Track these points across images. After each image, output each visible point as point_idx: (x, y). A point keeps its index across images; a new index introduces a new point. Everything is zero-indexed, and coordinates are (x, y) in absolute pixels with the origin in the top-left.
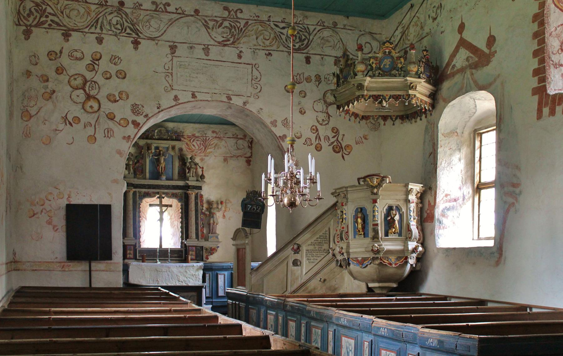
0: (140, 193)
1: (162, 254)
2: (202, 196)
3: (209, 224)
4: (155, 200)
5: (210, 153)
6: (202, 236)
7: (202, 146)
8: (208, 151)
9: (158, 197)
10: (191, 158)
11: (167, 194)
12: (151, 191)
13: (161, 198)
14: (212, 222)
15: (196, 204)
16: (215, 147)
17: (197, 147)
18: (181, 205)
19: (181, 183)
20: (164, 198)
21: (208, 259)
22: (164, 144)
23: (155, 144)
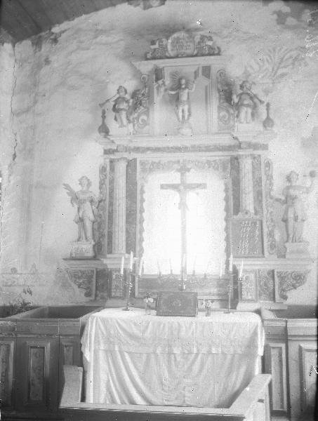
0: (142, 163)
1: (172, 298)
2: (268, 165)
3: (285, 221)
4: (174, 177)
5: (283, 75)
6: (272, 246)
7: (267, 65)
8: (280, 72)
9: (178, 170)
10: (242, 87)
11: (200, 166)
12: (165, 157)
13: (183, 170)
14: (291, 215)
15: (258, 182)
16: (293, 64)
17: (256, 67)
18: (226, 185)
19: (226, 140)
20: (189, 170)
21: (285, 298)
22: (189, 66)
23: (167, 65)
